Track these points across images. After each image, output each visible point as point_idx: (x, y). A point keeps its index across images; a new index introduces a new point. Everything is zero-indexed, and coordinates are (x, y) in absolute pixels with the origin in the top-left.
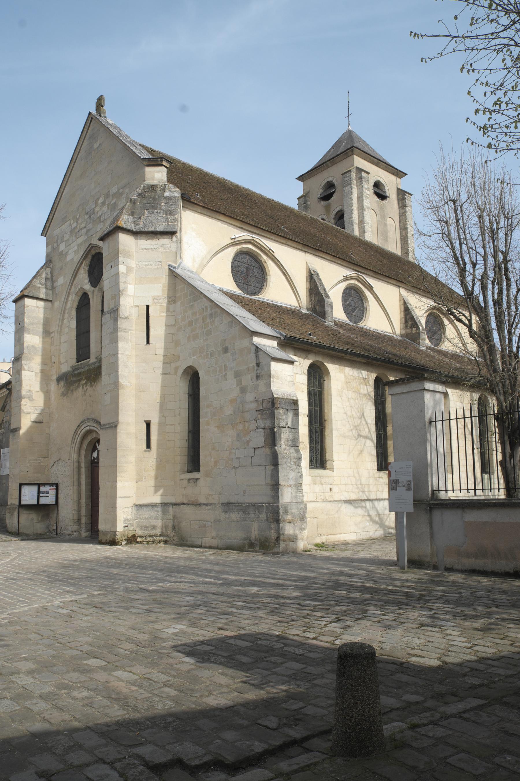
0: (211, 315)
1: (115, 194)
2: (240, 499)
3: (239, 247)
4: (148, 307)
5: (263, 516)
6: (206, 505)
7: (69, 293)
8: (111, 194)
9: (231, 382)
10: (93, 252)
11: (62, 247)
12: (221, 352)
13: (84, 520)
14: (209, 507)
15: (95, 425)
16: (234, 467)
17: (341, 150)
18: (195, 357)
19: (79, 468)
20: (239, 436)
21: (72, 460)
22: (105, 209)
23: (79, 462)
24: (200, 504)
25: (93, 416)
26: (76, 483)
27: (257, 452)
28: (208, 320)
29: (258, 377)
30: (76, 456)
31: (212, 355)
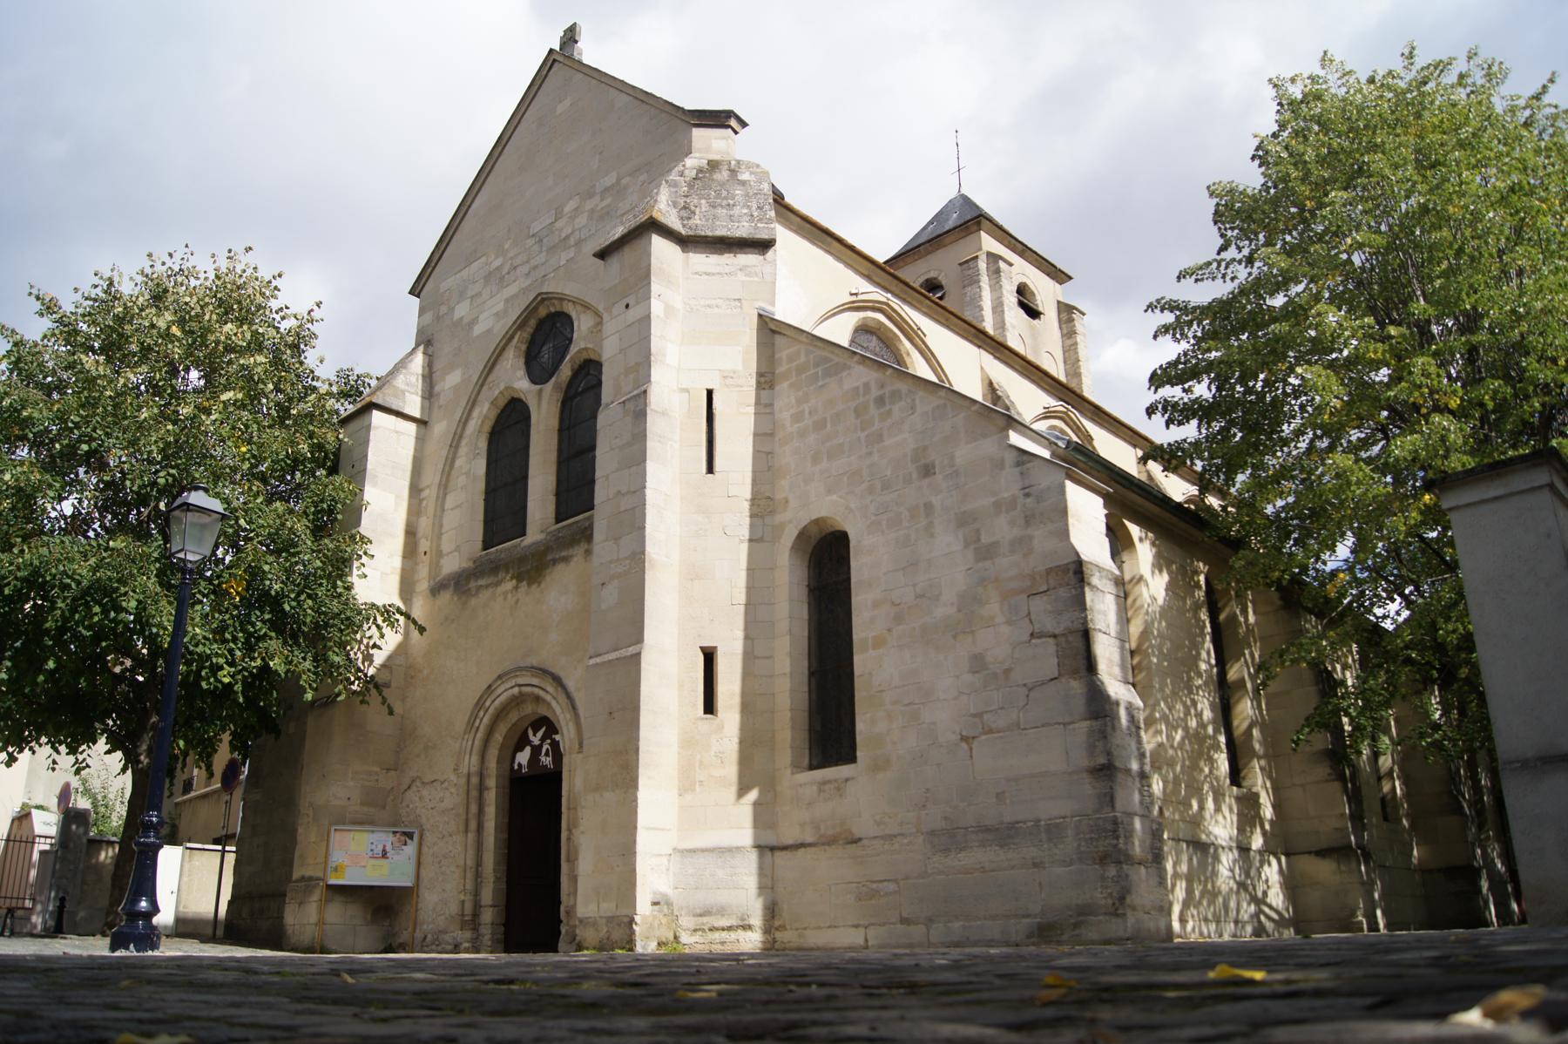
0: (880, 401)
1: (607, 190)
3: (862, 314)
4: (710, 393)
7: (473, 404)
8: (598, 190)
9: (947, 541)
10: (543, 312)
11: (462, 310)
12: (914, 476)
13: (487, 916)
15: (535, 681)
16: (964, 739)
17: (950, 224)
18: (834, 497)
19: (482, 788)
21: (465, 771)
22: (582, 220)
23: (481, 775)
25: (534, 661)
26: (473, 825)
28: (873, 411)
29: (1029, 520)
30: (475, 759)
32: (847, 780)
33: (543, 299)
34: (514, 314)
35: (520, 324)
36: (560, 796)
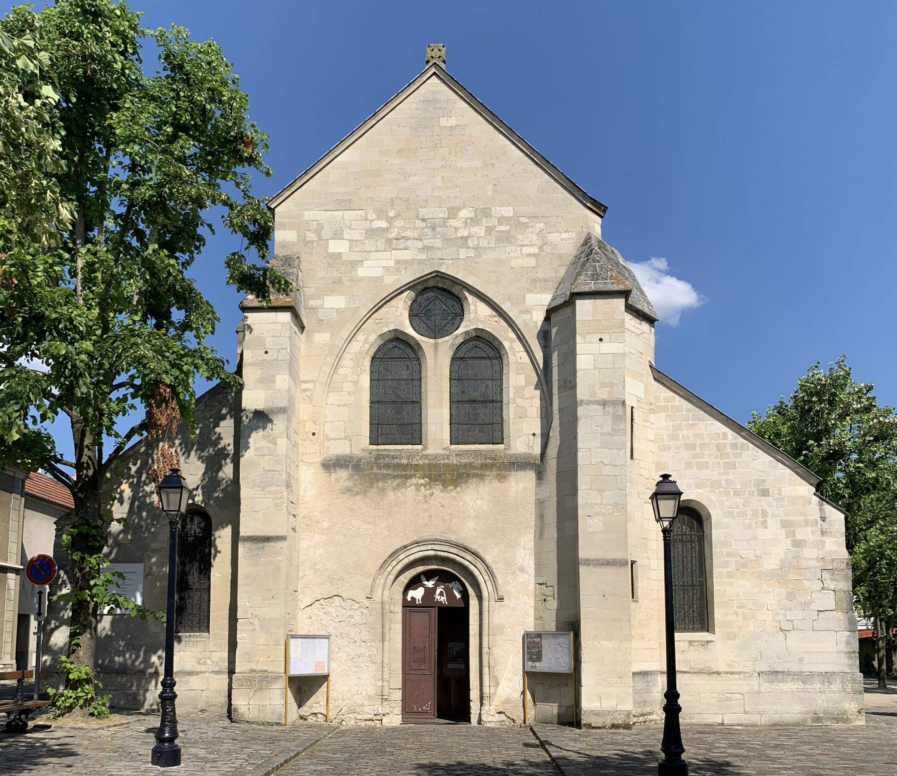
2: (795, 668)
5: (836, 686)
6: (727, 673)
10: (431, 284)
12: (756, 494)
14: (737, 676)
18: (701, 491)
20: (791, 596)
21: (379, 600)
24: (719, 673)
27: (821, 614)
28: (729, 450)
29: (823, 533)
31: (736, 493)
32: (708, 642)
33: (439, 275)
34: (409, 277)
35: (411, 286)
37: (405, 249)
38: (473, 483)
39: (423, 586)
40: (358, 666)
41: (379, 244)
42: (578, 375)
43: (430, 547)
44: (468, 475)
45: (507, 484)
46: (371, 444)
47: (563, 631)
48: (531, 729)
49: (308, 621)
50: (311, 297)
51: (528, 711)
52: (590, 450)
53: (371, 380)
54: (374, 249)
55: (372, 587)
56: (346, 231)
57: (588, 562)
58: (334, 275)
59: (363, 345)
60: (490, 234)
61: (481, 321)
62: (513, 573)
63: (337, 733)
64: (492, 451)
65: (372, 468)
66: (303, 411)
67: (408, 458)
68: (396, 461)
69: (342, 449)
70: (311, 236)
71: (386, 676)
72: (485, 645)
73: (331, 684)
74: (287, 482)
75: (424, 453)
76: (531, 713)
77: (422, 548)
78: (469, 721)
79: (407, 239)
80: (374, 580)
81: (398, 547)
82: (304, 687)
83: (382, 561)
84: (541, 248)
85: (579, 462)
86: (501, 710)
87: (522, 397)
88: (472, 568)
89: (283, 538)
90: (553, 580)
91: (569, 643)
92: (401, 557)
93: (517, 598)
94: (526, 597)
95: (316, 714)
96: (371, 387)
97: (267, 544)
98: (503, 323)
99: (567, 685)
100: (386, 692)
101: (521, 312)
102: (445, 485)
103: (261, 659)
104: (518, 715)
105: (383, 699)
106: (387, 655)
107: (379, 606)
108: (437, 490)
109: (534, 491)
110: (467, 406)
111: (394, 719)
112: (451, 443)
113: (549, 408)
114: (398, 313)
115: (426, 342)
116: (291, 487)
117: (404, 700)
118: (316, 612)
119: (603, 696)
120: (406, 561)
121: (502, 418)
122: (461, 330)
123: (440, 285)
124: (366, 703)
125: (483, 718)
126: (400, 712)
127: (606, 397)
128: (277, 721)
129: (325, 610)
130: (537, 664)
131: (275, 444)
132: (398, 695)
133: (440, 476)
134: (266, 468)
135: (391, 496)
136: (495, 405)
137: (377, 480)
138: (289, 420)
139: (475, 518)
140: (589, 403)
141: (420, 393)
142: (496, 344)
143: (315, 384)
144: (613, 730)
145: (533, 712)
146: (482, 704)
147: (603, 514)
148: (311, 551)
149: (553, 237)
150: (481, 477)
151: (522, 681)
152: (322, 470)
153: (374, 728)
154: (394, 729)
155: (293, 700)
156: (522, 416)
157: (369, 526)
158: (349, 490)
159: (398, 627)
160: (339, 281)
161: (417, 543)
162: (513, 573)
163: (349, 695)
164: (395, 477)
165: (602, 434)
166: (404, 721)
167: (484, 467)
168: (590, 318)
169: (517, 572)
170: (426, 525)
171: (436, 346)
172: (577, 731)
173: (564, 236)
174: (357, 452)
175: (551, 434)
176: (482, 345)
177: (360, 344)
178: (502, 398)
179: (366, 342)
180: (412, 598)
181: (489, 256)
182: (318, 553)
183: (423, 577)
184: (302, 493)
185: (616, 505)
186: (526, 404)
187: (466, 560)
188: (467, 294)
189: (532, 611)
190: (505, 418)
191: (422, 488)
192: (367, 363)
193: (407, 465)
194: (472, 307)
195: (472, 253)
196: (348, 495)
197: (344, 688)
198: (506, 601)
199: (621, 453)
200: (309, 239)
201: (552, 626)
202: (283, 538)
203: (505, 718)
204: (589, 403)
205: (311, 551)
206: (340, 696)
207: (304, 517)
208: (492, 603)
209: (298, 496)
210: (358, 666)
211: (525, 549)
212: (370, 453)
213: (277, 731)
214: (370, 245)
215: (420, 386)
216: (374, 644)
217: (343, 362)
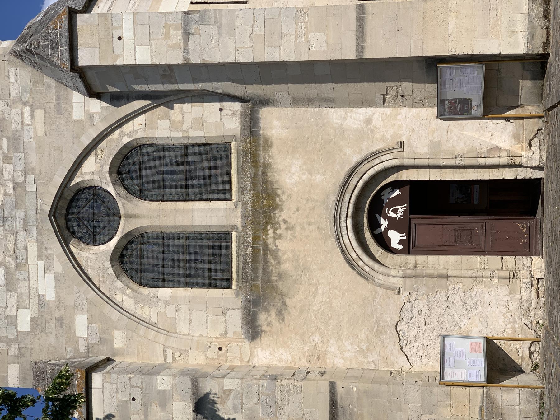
10: (62, 222)
33: (53, 213)
34: (55, 246)
35: (65, 243)
36: (429, 181)
37: (26, 249)
38: (273, 176)
39: (386, 231)
40: (476, 304)
41: (21, 277)
42: (157, 62)
43: (343, 224)
44: (265, 181)
45: (273, 139)
46: (230, 287)
47: (436, 75)
48: (549, 110)
49: (425, 359)
50: (76, 350)
51: (528, 114)
52: (237, 49)
53: (164, 287)
54: (26, 283)
55: (387, 288)
56: (8, 312)
57: (360, 49)
58: (53, 325)
59: (128, 295)
60: (11, 158)
61: (102, 167)
62: (372, 131)
63: (552, 329)
64: (239, 155)
65: (257, 286)
66: (195, 360)
67: (246, 247)
68: (249, 260)
69: (236, 318)
70: (14, 350)
71: (488, 273)
72: (452, 162)
73: (496, 336)
74: (272, 379)
75: (240, 229)
76: (531, 110)
77: (344, 232)
78: (539, 180)
79: (16, 247)
80: (380, 286)
81: (342, 259)
82: (499, 367)
83: (359, 277)
84: (25, 104)
85: (251, 60)
86: (527, 144)
87: (181, 122)
88: (366, 177)
89: (332, 386)
90: (380, 86)
91: (450, 68)
92: (354, 256)
93: (400, 127)
94: (399, 117)
95: (531, 354)
96: (171, 286)
97: (339, 404)
98: (103, 144)
99: (499, 70)
100: (505, 274)
101: (92, 124)
102: (275, 207)
103: (467, 414)
104: (532, 125)
105: (513, 276)
106: (463, 273)
107: (408, 280)
108: (280, 216)
109: (282, 109)
110: (191, 182)
111: (537, 265)
112: (230, 199)
113: (193, 94)
114: (93, 257)
115: (124, 227)
116: (276, 376)
117: (515, 253)
118: (414, 350)
119: (512, 29)
120: (359, 251)
121: (203, 144)
122: (111, 189)
123: (64, 212)
124: (518, 296)
125: (536, 164)
126: (529, 259)
127: (180, 33)
128: (538, 398)
129: (413, 341)
130: (474, 103)
131: (230, 391)
132: (509, 260)
133: (264, 212)
134: (255, 401)
135: (287, 266)
136: (190, 151)
137: (269, 281)
138: (205, 375)
139: (311, 174)
140: (186, 50)
141: (178, 233)
142: (125, 152)
143: (168, 347)
144: (551, 17)
145: (530, 108)
146: (520, 166)
147: (307, 33)
148: (347, 355)
149: (14, 93)
150: (266, 167)
151: (494, 121)
152: (258, 341)
153: (547, 288)
154: (549, 266)
155: (514, 379)
156: (201, 122)
157: (320, 291)
158: (280, 313)
159: (432, 259)
160: (60, 320)
161: (338, 238)
162: (372, 131)
163: (509, 315)
164: (266, 262)
165: (220, 35)
166: (539, 253)
167: (255, 163)
168: (97, 50)
169: (371, 126)
170: (318, 228)
171: (128, 216)
172: (551, 58)
173: (12, 79)
174: (240, 302)
175: (220, 91)
176: (127, 167)
177: (126, 298)
178: (182, 145)
179: (123, 292)
180: (400, 243)
181: (33, 159)
182: (349, 347)
183: (377, 232)
184: (283, 364)
185: (296, 19)
186: (188, 119)
187: (357, 184)
188: (73, 183)
189: (414, 110)
190: (203, 141)
191: (278, 232)
192: (146, 291)
193: (253, 248)
194: (87, 177)
195: (31, 178)
196: (285, 314)
197: (501, 321)
198: (404, 139)
199: (240, 14)
200: (17, 352)
201: (432, 88)
202: (332, 386)
203: (536, 140)
204: (186, 50)
205: (347, 355)
206: (509, 326)
207: (309, 362)
208: (405, 154)
209: (286, 368)
210: (476, 304)
211: (345, 118)
212: (241, 288)
213: (550, 398)
214: (23, 287)
215: (170, 233)
216: (451, 287)
217: (145, 316)
